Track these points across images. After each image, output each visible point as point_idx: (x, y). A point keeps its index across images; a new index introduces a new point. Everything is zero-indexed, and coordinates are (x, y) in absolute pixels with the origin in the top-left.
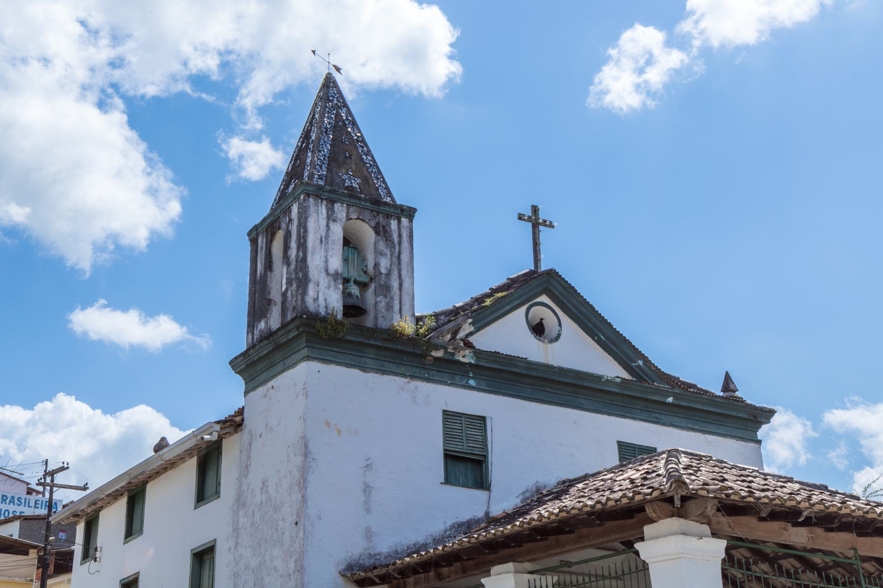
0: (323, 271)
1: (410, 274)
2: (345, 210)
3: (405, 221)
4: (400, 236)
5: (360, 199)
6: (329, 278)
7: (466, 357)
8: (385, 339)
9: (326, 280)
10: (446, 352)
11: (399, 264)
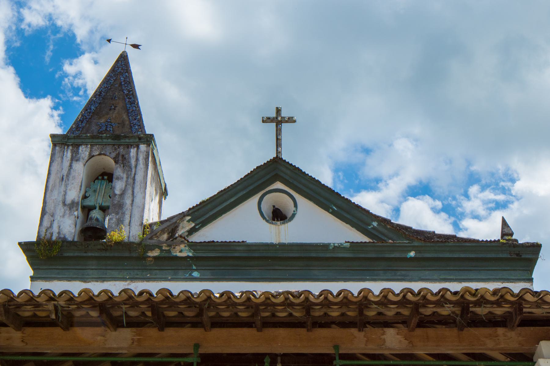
0: (61, 204)
1: (142, 190)
2: (88, 150)
3: (143, 147)
4: (137, 160)
6: (65, 208)
7: (182, 251)
8: (100, 250)
9: (63, 210)
10: (162, 251)
11: (134, 183)
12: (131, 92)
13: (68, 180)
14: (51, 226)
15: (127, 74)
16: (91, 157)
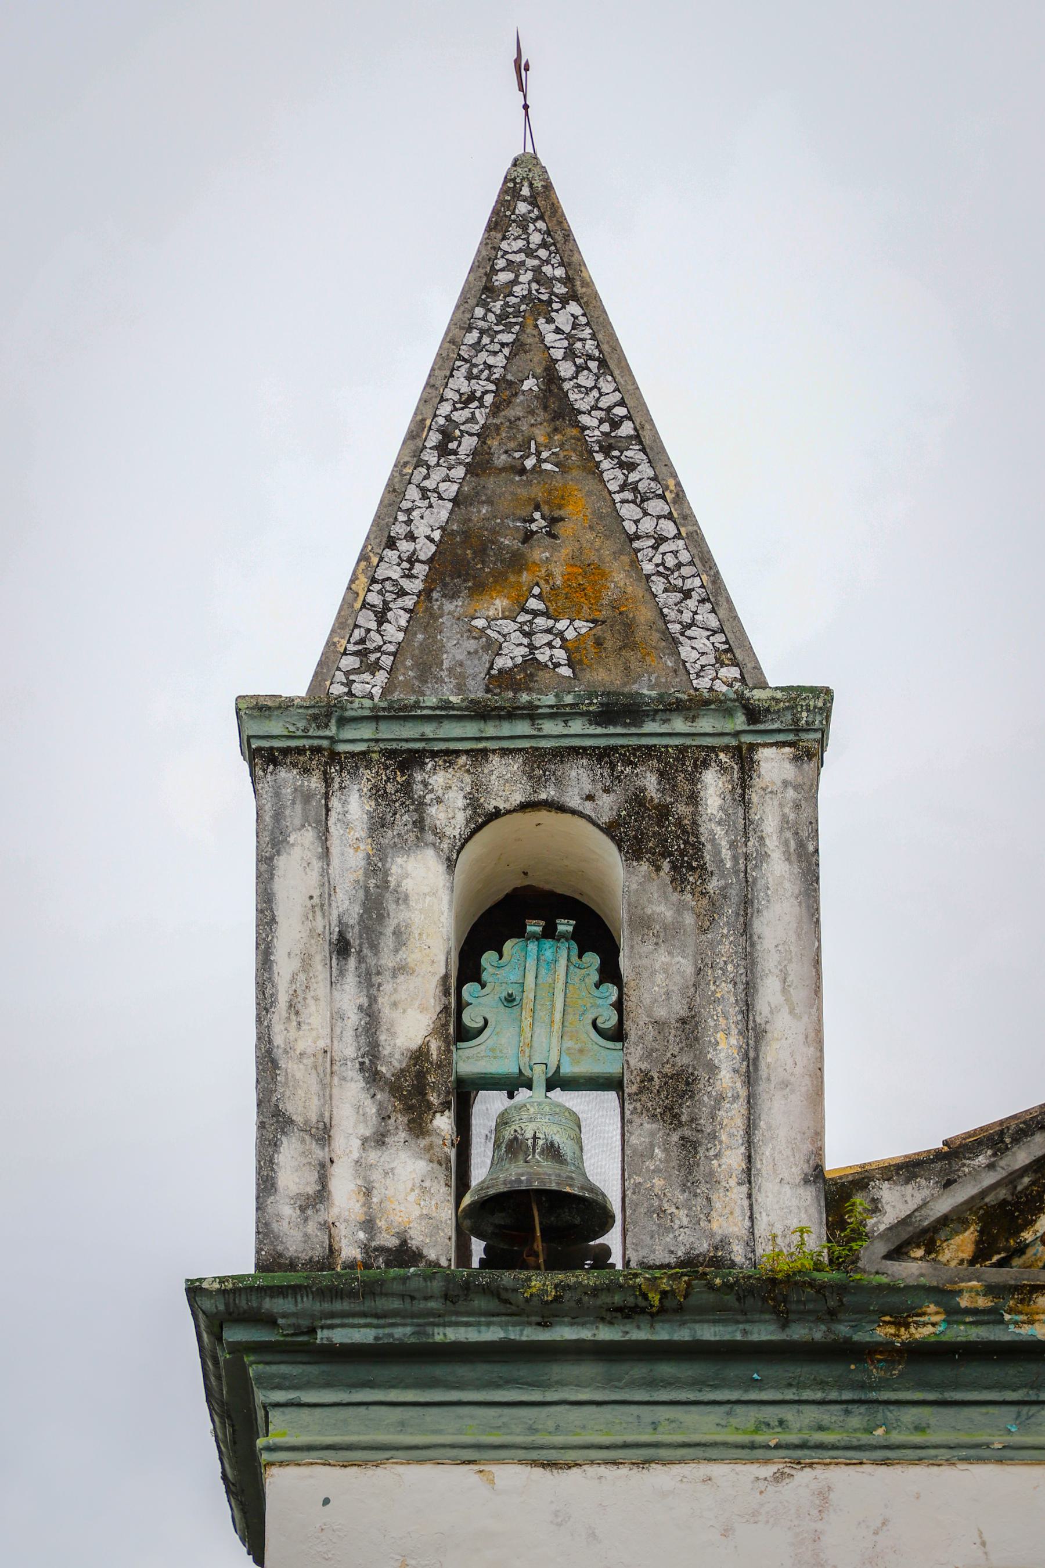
1: (800, 994)
5: (532, 714)
12: (626, 429)
13: (375, 947)
14: (322, 1195)
15: (574, 308)
16: (482, 818)
